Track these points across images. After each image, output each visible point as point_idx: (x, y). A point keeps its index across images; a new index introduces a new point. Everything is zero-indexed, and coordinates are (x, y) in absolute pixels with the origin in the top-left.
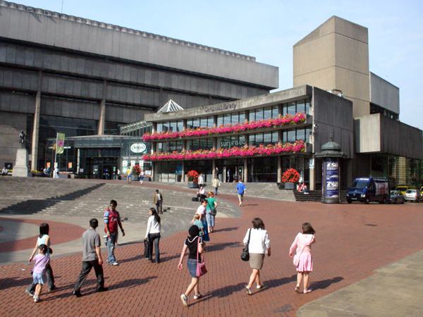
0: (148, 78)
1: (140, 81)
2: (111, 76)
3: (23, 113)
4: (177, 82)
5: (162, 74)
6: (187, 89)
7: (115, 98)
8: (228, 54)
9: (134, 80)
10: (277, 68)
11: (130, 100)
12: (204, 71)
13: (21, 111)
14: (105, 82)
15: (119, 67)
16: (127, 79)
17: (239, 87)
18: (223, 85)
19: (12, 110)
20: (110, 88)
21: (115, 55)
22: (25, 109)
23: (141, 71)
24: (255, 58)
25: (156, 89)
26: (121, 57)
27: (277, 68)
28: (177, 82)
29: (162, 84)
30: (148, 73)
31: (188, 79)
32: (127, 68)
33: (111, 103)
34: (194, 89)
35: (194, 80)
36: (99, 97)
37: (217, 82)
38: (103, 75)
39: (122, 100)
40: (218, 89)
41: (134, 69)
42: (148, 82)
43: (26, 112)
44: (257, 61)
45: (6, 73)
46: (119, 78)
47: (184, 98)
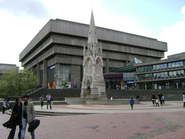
0: (123, 49)
2: (111, 49)
3: (79, 65)
4: (133, 51)
5: (128, 48)
6: (136, 53)
7: (111, 58)
9: (118, 50)
10: (166, 43)
11: (117, 59)
12: (142, 46)
13: (79, 64)
14: (108, 52)
15: (113, 45)
16: (116, 50)
18: (148, 51)
19: (76, 64)
20: (109, 54)
21: (112, 41)
22: (80, 64)
23: (120, 47)
24: (157, 40)
25: (126, 53)
26: (114, 41)
27: (166, 43)
28: (133, 51)
29: (128, 52)
30: (123, 47)
31: (136, 49)
32: (116, 46)
33: (110, 59)
34: (139, 53)
35: (138, 49)
36: (106, 58)
37: (146, 50)
38: (108, 49)
39: (114, 58)
40: (147, 52)
41: (118, 46)
42: (123, 51)
43: (80, 64)
45: (74, 49)
46: (113, 50)
47: (142, 58)
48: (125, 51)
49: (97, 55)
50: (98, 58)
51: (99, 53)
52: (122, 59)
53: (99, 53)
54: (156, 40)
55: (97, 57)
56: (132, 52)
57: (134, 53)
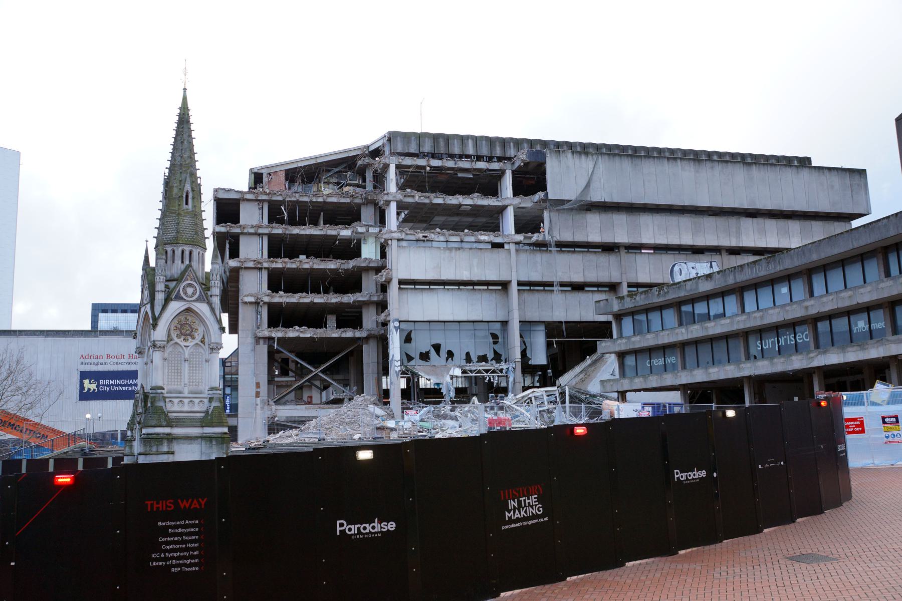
1: (580, 238)
5: (621, 219)
6: (674, 240)
8: (749, 160)
10: (864, 171)
17: (782, 223)
24: (809, 160)
29: (621, 237)
31: (673, 220)
35: (685, 221)
36: (504, 278)
37: (732, 221)
42: (594, 237)
44: (813, 164)
48: (608, 238)
49: (178, 298)
50: (188, 310)
51: (190, 291)
52: (592, 277)
53: (190, 291)
54: (804, 162)
55: (175, 307)
56: (647, 238)
57: (662, 240)
